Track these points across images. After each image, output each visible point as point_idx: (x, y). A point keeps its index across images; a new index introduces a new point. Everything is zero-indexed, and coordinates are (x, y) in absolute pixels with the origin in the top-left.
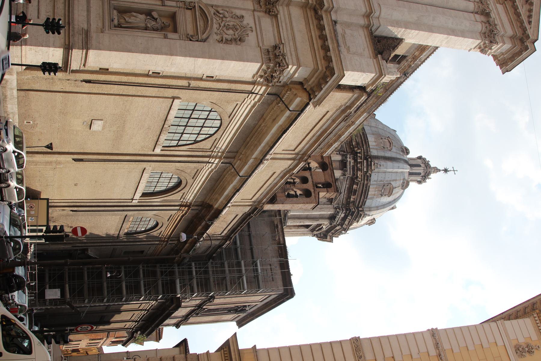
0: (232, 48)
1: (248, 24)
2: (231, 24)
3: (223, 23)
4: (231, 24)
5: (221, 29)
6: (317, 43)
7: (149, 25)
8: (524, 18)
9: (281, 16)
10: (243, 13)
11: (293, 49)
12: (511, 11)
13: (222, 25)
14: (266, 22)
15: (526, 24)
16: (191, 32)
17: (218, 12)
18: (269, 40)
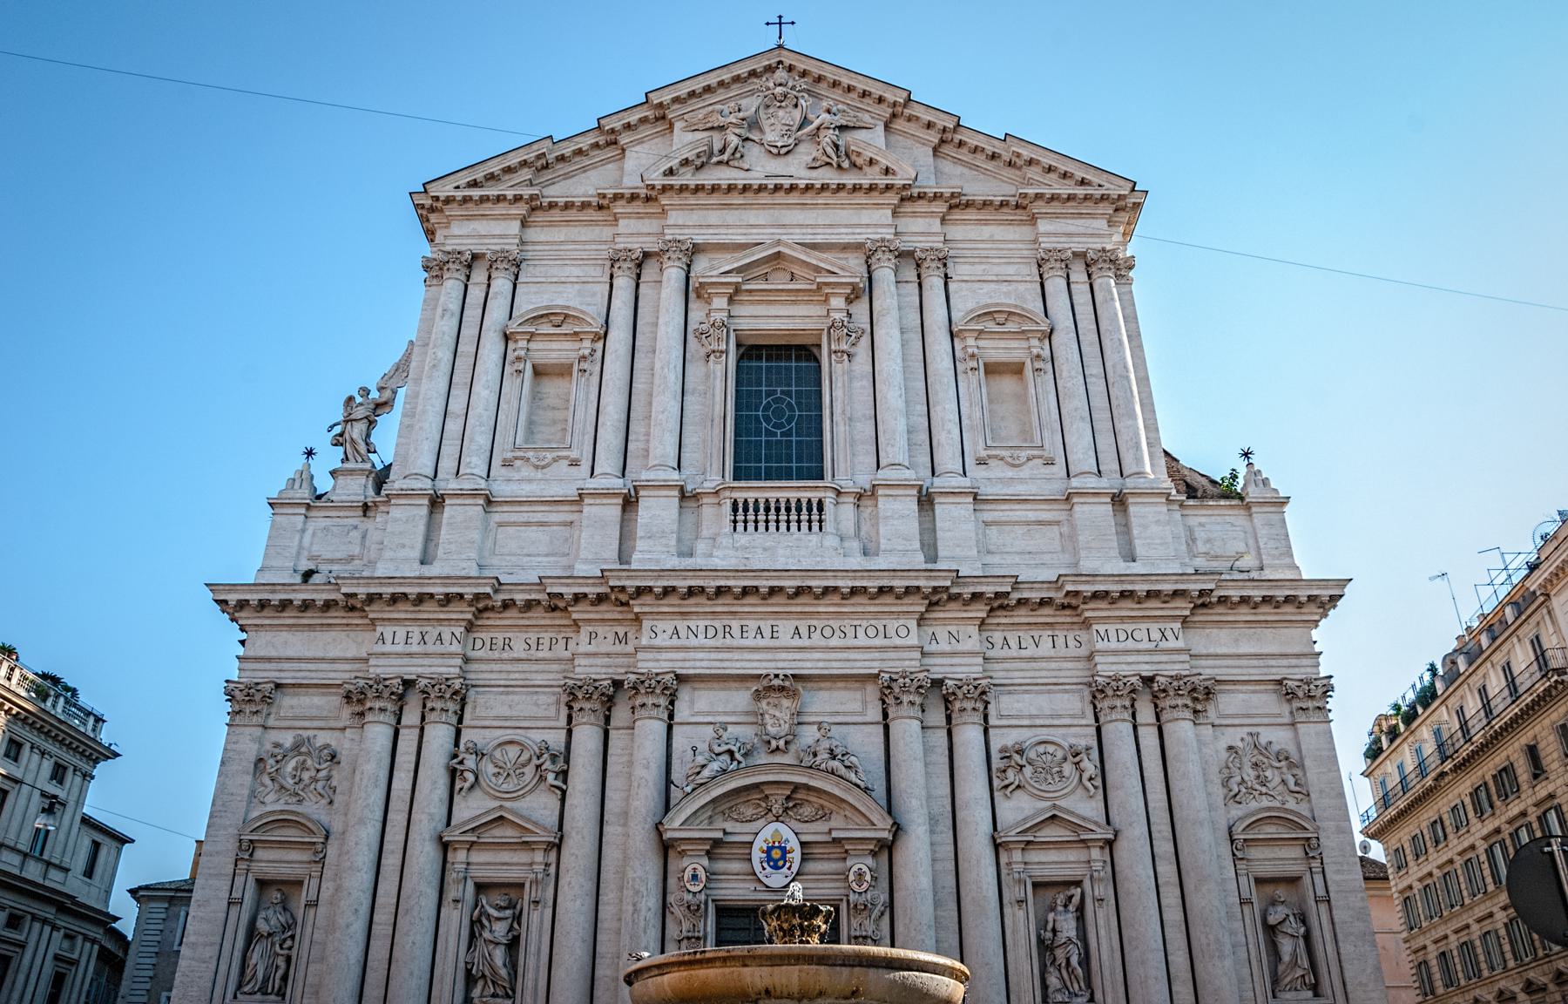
0: (1314, 775)
1: (1242, 739)
2: (1253, 773)
4: (1253, 773)
5: (1271, 793)
6: (1264, 614)
7: (1302, 930)
8: (1081, 191)
9: (1222, 674)
11: (1285, 662)
12: (1055, 207)
13: (1264, 790)
14: (1229, 703)
15: (1098, 193)
16: (1297, 852)
17: (1236, 795)
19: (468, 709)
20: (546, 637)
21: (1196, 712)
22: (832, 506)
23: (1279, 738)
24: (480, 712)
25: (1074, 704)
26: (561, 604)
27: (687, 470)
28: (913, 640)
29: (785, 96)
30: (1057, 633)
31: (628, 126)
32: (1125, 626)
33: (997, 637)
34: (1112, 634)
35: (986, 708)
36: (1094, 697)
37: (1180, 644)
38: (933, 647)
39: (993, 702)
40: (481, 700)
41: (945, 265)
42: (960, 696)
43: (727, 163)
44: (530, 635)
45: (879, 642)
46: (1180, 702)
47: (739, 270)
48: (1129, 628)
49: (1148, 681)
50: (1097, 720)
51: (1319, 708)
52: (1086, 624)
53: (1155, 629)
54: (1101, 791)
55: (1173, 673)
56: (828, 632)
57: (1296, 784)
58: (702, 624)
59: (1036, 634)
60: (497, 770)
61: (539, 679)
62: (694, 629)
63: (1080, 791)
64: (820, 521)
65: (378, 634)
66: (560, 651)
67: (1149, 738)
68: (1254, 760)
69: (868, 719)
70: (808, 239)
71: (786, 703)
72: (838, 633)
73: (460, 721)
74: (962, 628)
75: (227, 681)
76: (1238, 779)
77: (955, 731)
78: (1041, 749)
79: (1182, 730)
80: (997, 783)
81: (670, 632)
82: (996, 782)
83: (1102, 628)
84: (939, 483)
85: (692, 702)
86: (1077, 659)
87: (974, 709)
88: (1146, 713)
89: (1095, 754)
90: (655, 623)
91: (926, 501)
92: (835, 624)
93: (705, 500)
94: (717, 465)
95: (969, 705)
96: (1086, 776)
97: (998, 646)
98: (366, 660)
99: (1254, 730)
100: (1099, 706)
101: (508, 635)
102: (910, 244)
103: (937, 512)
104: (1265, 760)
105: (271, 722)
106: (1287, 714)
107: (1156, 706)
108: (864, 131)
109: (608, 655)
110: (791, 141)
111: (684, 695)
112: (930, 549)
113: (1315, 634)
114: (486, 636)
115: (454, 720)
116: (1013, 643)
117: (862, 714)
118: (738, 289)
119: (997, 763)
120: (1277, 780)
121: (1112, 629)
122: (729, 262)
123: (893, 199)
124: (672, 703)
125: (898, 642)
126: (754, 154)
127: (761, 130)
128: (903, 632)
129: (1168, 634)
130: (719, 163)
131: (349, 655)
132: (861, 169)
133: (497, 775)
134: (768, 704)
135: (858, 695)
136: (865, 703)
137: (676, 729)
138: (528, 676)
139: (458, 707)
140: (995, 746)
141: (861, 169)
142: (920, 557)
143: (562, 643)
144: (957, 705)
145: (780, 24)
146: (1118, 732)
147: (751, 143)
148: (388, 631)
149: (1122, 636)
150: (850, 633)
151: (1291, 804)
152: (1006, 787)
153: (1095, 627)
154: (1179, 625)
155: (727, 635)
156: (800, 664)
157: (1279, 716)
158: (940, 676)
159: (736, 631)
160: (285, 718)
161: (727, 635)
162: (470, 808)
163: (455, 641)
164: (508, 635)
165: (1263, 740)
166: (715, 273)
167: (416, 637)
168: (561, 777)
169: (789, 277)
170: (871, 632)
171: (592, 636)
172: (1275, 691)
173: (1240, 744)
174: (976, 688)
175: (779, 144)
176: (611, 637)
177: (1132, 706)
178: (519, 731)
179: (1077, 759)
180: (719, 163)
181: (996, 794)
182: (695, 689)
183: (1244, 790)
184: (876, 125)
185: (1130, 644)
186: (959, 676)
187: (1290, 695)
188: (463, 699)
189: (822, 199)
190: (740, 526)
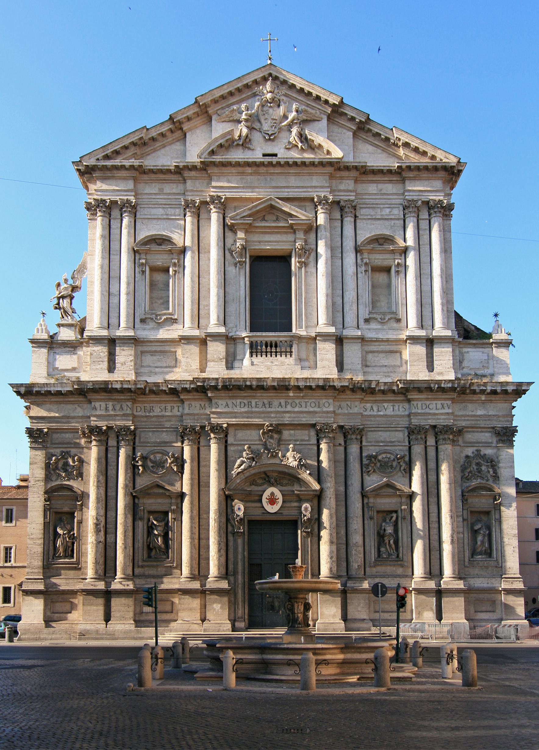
1: (473, 453)
2: (475, 468)
3: (477, 473)
10: (463, 455)
13: (479, 475)
18: (486, 436)
19: (137, 439)
20: (169, 406)
21: (453, 441)
22: (296, 345)
23: (489, 452)
24: (142, 440)
25: (401, 436)
26: (176, 393)
27: (230, 325)
28: (331, 409)
29: (273, 100)
30: (395, 404)
31: (189, 119)
32: (426, 402)
33: (368, 405)
34: (419, 405)
35: (361, 438)
36: (409, 433)
37: (450, 411)
38: (340, 411)
39: (364, 434)
40: (143, 435)
41: (355, 209)
42: (351, 433)
43: (242, 145)
44: (162, 405)
45: (316, 409)
46: (446, 436)
47: (249, 216)
48: (428, 403)
49: (434, 427)
50: (409, 443)
51: (510, 440)
52: (409, 401)
53: (439, 402)
54: (408, 475)
55: (445, 424)
56: (294, 404)
57: (494, 473)
58: (238, 401)
59: (386, 405)
60: (152, 465)
61: (168, 425)
62: (235, 403)
63: (400, 474)
64: (291, 352)
65: (93, 406)
66: (176, 412)
67: (432, 453)
68: (477, 461)
69: (311, 443)
70: (284, 195)
71: (276, 436)
72: (298, 405)
73: (134, 443)
74: (353, 403)
75: (27, 428)
76: (468, 470)
77: (348, 447)
78: (384, 456)
79: (447, 449)
80: (364, 470)
81: (224, 404)
82: (364, 469)
83: (415, 403)
84: (346, 333)
85: (235, 435)
86: (403, 416)
87: (356, 439)
88: (431, 441)
89: (407, 459)
90: (218, 401)
91: (339, 341)
92: (297, 401)
93: (238, 341)
94: (243, 323)
95: (354, 437)
96: (402, 468)
97: (368, 410)
98: (89, 417)
99: (479, 448)
100: (411, 438)
101: (151, 405)
102: (338, 197)
103: (344, 347)
104: (482, 462)
105: (48, 446)
106: (495, 441)
107: (436, 438)
108: (317, 122)
109: (197, 414)
110: (276, 130)
111: (231, 431)
112: (340, 365)
113: (514, 404)
114: (142, 406)
115: (132, 444)
116: (375, 408)
117: (309, 440)
118: (250, 225)
119: (365, 461)
120: (486, 470)
121: (420, 403)
122: (244, 210)
123: (329, 169)
124: (226, 436)
125: (325, 409)
126: (257, 137)
127: (260, 122)
128: (327, 405)
129: (445, 405)
130: (238, 145)
131: (80, 415)
132: (314, 149)
133: (152, 467)
134: (268, 436)
135: (306, 432)
136: (309, 436)
137: (229, 448)
138: (162, 423)
139: (133, 438)
140: (364, 454)
141: (314, 149)
142: (335, 370)
143: (176, 408)
144: (349, 437)
145: (270, 40)
146: (418, 449)
147: (255, 131)
148: (97, 404)
149: (424, 407)
150: (303, 405)
151: (490, 483)
152: (369, 472)
153: (412, 402)
154: (451, 402)
155: (250, 406)
156: (282, 419)
157: (491, 443)
158: (342, 424)
159: (253, 404)
160: (55, 444)
161: (250, 406)
162: (142, 482)
163: (128, 409)
164: (151, 405)
165: (482, 453)
166: (238, 217)
167: (110, 407)
168: (180, 468)
169: (275, 218)
170: (313, 405)
171: (190, 406)
172: (490, 432)
173: (472, 455)
174: (358, 429)
175: (270, 133)
176: (198, 406)
177: (426, 437)
178: (159, 448)
179: (399, 461)
180: (238, 145)
181: (364, 474)
182: (236, 430)
183: (470, 475)
184: (322, 118)
185: (428, 411)
186: (351, 424)
187: (498, 434)
188: (135, 434)
189: (292, 170)
190: (254, 356)
